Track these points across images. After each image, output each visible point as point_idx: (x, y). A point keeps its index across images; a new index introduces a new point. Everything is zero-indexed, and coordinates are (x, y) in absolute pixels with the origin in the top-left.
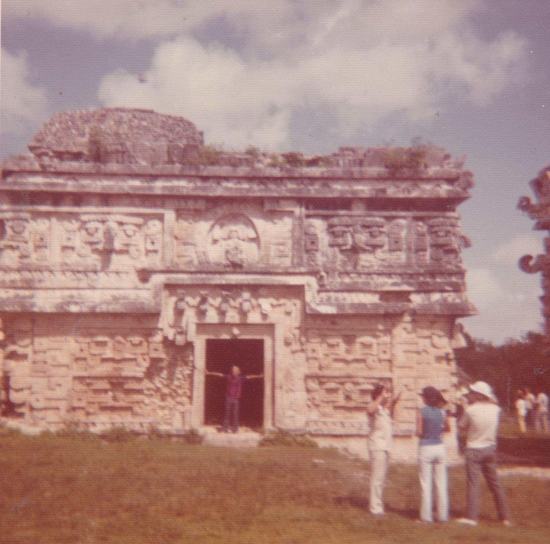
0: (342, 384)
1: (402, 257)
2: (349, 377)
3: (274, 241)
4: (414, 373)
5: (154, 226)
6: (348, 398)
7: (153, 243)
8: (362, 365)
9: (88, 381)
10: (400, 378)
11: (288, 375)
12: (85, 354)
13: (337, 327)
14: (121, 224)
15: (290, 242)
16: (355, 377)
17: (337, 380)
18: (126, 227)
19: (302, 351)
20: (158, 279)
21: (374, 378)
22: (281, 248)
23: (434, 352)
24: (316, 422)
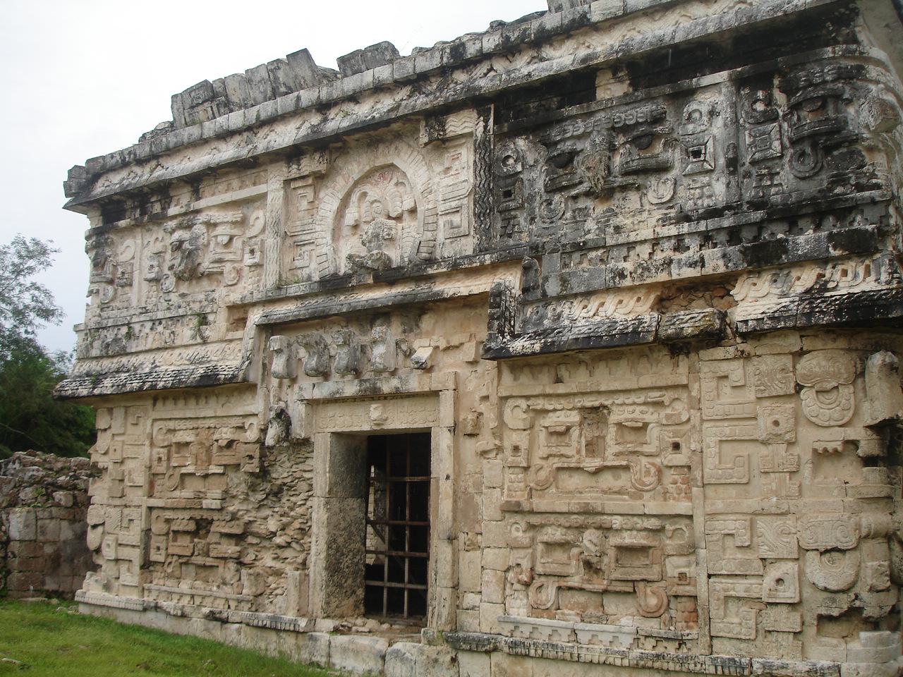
0: (581, 528)
1: (719, 190)
2: (587, 512)
3: (441, 208)
4: (752, 503)
5: (259, 218)
6: (588, 565)
7: (252, 252)
8: (624, 480)
9: (169, 515)
10: (712, 515)
11: (465, 507)
12: (161, 469)
13: (561, 389)
14: (211, 225)
15: (468, 204)
16: (603, 514)
17: (562, 520)
18: (219, 230)
19: (499, 449)
20: (255, 316)
21: (645, 515)
22: (456, 219)
23: (810, 438)
24: (517, 625)
